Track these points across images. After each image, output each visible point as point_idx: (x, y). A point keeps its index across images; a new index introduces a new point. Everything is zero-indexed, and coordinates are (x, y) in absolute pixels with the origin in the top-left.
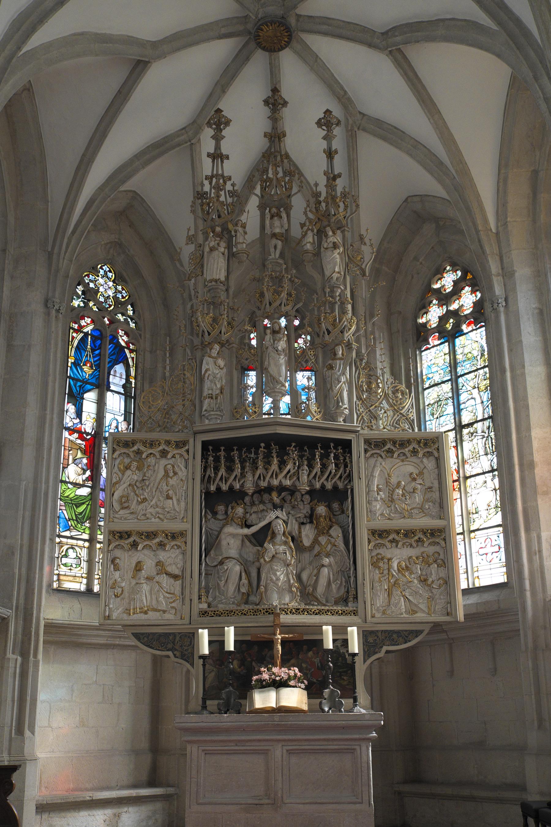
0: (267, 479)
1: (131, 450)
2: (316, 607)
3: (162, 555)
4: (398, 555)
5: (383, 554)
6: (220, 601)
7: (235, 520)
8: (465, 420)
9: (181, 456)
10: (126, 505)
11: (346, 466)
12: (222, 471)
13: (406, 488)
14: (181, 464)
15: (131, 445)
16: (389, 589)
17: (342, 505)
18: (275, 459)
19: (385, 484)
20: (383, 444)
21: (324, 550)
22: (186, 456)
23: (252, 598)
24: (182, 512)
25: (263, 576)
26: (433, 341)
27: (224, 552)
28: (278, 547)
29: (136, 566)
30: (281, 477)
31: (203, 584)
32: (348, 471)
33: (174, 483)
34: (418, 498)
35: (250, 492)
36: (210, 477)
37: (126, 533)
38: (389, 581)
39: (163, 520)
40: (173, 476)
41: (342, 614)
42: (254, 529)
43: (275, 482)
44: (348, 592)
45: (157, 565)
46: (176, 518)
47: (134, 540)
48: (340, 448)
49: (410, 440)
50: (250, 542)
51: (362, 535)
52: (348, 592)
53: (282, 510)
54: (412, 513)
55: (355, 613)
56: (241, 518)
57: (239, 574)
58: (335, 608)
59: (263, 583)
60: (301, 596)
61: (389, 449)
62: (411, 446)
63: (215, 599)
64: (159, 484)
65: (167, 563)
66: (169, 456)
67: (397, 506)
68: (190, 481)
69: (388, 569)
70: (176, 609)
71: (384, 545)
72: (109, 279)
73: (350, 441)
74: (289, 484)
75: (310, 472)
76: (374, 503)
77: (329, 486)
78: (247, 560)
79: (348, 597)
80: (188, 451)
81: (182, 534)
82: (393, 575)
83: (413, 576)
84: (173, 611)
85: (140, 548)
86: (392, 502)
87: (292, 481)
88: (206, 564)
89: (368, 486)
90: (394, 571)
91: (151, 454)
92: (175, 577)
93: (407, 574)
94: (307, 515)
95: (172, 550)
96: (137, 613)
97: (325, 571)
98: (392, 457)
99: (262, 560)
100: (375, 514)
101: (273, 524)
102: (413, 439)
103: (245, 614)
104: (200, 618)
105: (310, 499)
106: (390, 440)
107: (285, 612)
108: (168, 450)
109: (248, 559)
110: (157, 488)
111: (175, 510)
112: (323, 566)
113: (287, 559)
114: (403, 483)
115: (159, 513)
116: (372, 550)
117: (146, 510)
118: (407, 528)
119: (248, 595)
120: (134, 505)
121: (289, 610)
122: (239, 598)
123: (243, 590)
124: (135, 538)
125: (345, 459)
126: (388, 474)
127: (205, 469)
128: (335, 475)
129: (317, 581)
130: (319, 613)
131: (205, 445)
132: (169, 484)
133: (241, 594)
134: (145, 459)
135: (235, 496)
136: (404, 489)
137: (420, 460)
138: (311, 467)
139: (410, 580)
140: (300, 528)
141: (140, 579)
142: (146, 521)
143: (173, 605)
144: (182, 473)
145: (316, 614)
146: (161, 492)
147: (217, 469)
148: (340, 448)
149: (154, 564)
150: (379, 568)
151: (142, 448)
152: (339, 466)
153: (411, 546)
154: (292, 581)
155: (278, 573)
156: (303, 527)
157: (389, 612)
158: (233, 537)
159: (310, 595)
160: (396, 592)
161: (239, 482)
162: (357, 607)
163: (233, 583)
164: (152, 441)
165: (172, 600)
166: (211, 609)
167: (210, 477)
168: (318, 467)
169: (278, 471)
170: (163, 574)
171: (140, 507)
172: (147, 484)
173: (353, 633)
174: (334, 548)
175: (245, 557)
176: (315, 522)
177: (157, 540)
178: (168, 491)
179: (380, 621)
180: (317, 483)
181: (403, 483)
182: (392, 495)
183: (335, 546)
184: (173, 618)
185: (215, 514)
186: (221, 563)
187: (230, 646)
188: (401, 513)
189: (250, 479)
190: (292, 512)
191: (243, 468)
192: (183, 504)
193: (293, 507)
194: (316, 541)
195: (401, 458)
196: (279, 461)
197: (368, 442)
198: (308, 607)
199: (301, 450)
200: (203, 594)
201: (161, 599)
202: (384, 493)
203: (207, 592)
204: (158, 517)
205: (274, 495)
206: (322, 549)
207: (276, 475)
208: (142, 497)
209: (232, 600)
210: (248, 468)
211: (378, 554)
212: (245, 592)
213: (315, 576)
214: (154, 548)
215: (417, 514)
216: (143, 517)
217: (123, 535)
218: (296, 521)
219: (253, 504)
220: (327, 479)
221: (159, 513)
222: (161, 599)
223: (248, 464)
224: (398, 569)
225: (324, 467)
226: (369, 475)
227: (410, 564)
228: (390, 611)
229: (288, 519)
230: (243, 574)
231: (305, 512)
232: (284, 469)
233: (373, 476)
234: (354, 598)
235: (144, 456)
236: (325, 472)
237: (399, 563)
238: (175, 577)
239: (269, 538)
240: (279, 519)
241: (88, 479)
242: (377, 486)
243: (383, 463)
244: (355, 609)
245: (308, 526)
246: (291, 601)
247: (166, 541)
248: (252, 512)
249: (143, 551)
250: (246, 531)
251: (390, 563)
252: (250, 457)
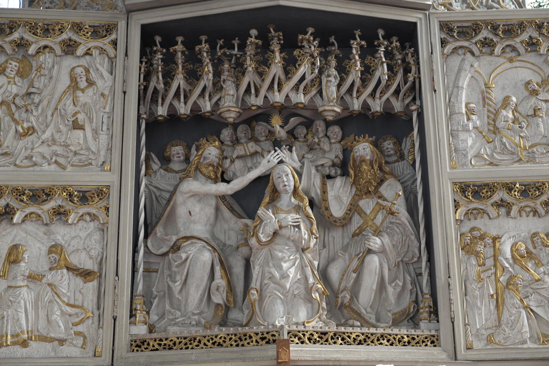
0: (263, 92)
1: (8, 39)
2: (358, 330)
3: (61, 233)
5: (483, 230)
6: (172, 320)
7: (203, 170)
9: (102, 51)
11: (407, 71)
13: (519, 109)
14: (100, 64)
15: (8, 30)
16: (497, 293)
17: (400, 144)
18: (277, 54)
19: (481, 102)
20: (475, 30)
21: (370, 223)
22: (111, 51)
23: (234, 315)
24: (103, 153)
25: (256, 271)
27: (182, 229)
28: (284, 216)
29: (9, 254)
30: (288, 87)
31: (140, 287)
32: (411, 79)
33: (90, 101)
35: (231, 117)
36: (156, 91)
38: (497, 280)
39: (64, 168)
40: (87, 87)
41: (409, 342)
42: (239, 183)
43: (278, 98)
44: (416, 302)
45: (50, 252)
46: (91, 164)
47: (7, 205)
48: (395, 39)
49: (522, 23)
50: (232, 210)
51: (443, 193)
52: (416, 302)
53: (290, 150)
54: (533, 152)
55: (434, 341)
56: (213, 166)
57: (210, 266)
58: (396, 331)
59: (255, 283)
60: (328, 311)
61: (485, 39)
62: (525, 33)
63: (162, 317)
64: (60, 100)
65: (71, 248)
66: (80, 51)
67: (504, 140)
68: (119, 95)
69: (494, 256)
70: (85, 338)
71: (484, 212)
73: (415, 24)
74: (303, 101)
76: (462, 136)
77: (377, 106)
78: (225, 245)
80: (114, 43)
81: (101, 193)
82: (504, 268)
83: (542, 269)
84: (80, 341)
85: (17, 218)
86: (494, 133)
87: (308, 97)
88: (147, 251)
89: (449, 104)
90: (506, 259)
91: (45, 47)
92: (86, 275)
93: (530, 265)
94: (337, 161)
95: (81, 223)
96: (7, 345)
97: (374, 261)
98: (492, 53)
99: (253, 241)
100: (465, 156)
101: (275, 175)
102: (529, 22)
103: (220, 345)
104: (131, 354)
105: (340, 134)
106: (486, 23)
107: (300, 339)
108: (78, 40)
109: (228, 243)
110: (56, 109)
111: (88, 149)
112: (370, 251)
113: (301, 238)
114: (514, 99)
115: (57, 155)
116: (461, 221)
117: (32, 149)
118: (528, 180)
119: (227, 309)
121: (307, 335)
122: (209, 313)
123: (218, 299)
124: (8, 200)
125: (404, 60)
126: (485, 84)
127: (147, 76)
128: (388, 87)
129: (358, 282)
130: (364, 341)
131: (148, 33)
132: (78, 101)
133: (213, 307)
134: (33, 56)
135: (204, 125)
136: (515, 110)
137: (543, 58)
138: (343, 71)
139: (537, 277)
140: (324, 184)
141: (15, 278)
142: (31, 169)
143: (80, 328)
144: (104, 82)
145: (360, 343)
146: (62, 117)
147: (168, 76)
148: (395, 39)
149: (44, 250)
150: (477, 254)
151: (28, 37)
152: (395, 70)
153: (535, 212)
154: (311, 280)
155: (285, 265)
156: (329, 183)
157: (499, 338)
158: (199, 201)
159: (346, 307)
160: (512, 300)
161: (210, 99)
162: (437, 330)
163: (198, 286)
164: (48, 25)
165: (77, 320)
166: (154, 335)
167: (156, 91)
168: (355, 74)
169: (283, 77)
170: (61, 268)
171: (21, 143)
172: (37, 100)
174: (390, 218)
175: (222, 237)
176: (352, 172)
177: (52, 204)
178: (76, 113)
179: (483, 357)
180: (355, 101)
181: (514, 99)
182: (494, 121)
183: (392, 213)
184: (78, 354)
185: (165, 160)
186: (176, 248)
188: (513, 154)
189: (231, 92)
190: (309, 156)
191: (217, 74)
192: (104, 138)
193: (311, 149)
194: (354, 208)
195: (508, 56)
196: (284, 59)
197: (446, 27)
198: (342, 329)
199: (324, 44)
200: (139, 307)
201: (56, 316)
202: (479, 118)
203: (148, 304)
204: (56, 162)
205: (276, 122)
206: (366, 222)
207: (280, 85)
208: (25, 125)
209: (196, 317)
210: (226, 73)
211: (473, 229)
212: (221, 302)
213: (354, 271)
214: (45, 218)
215: (543, 154)
216: (26, 162)
218: (317, 171)
219: (236, 142)
220: (373, 95)
221: (57, 155)
222: (56, 316)
223: (226, 66)
224: (513, 257)
225: (367, 71)
226: (451, 85)
227: (535, 248)
228: (501, 336)
229: (302, 167)
230: (218, 268)
231: (332, 156)
232: (294, 74)
233: (458, 87)
234: (430, 313)
235: (32, 50)
236: (370, 80)
237: (514, 245)
238: (86, 275)
239: (267, 199)
240: (285, 166)
242: (467, 105)
243: (476, 65)
244: (433, 333)
245: (339, 181)
246: (310, 318)
247: (68, 206)
248: (234, 156)
249: (24, 226)
250: (223, 188)
251: (497, 244)
252: (231, 56)
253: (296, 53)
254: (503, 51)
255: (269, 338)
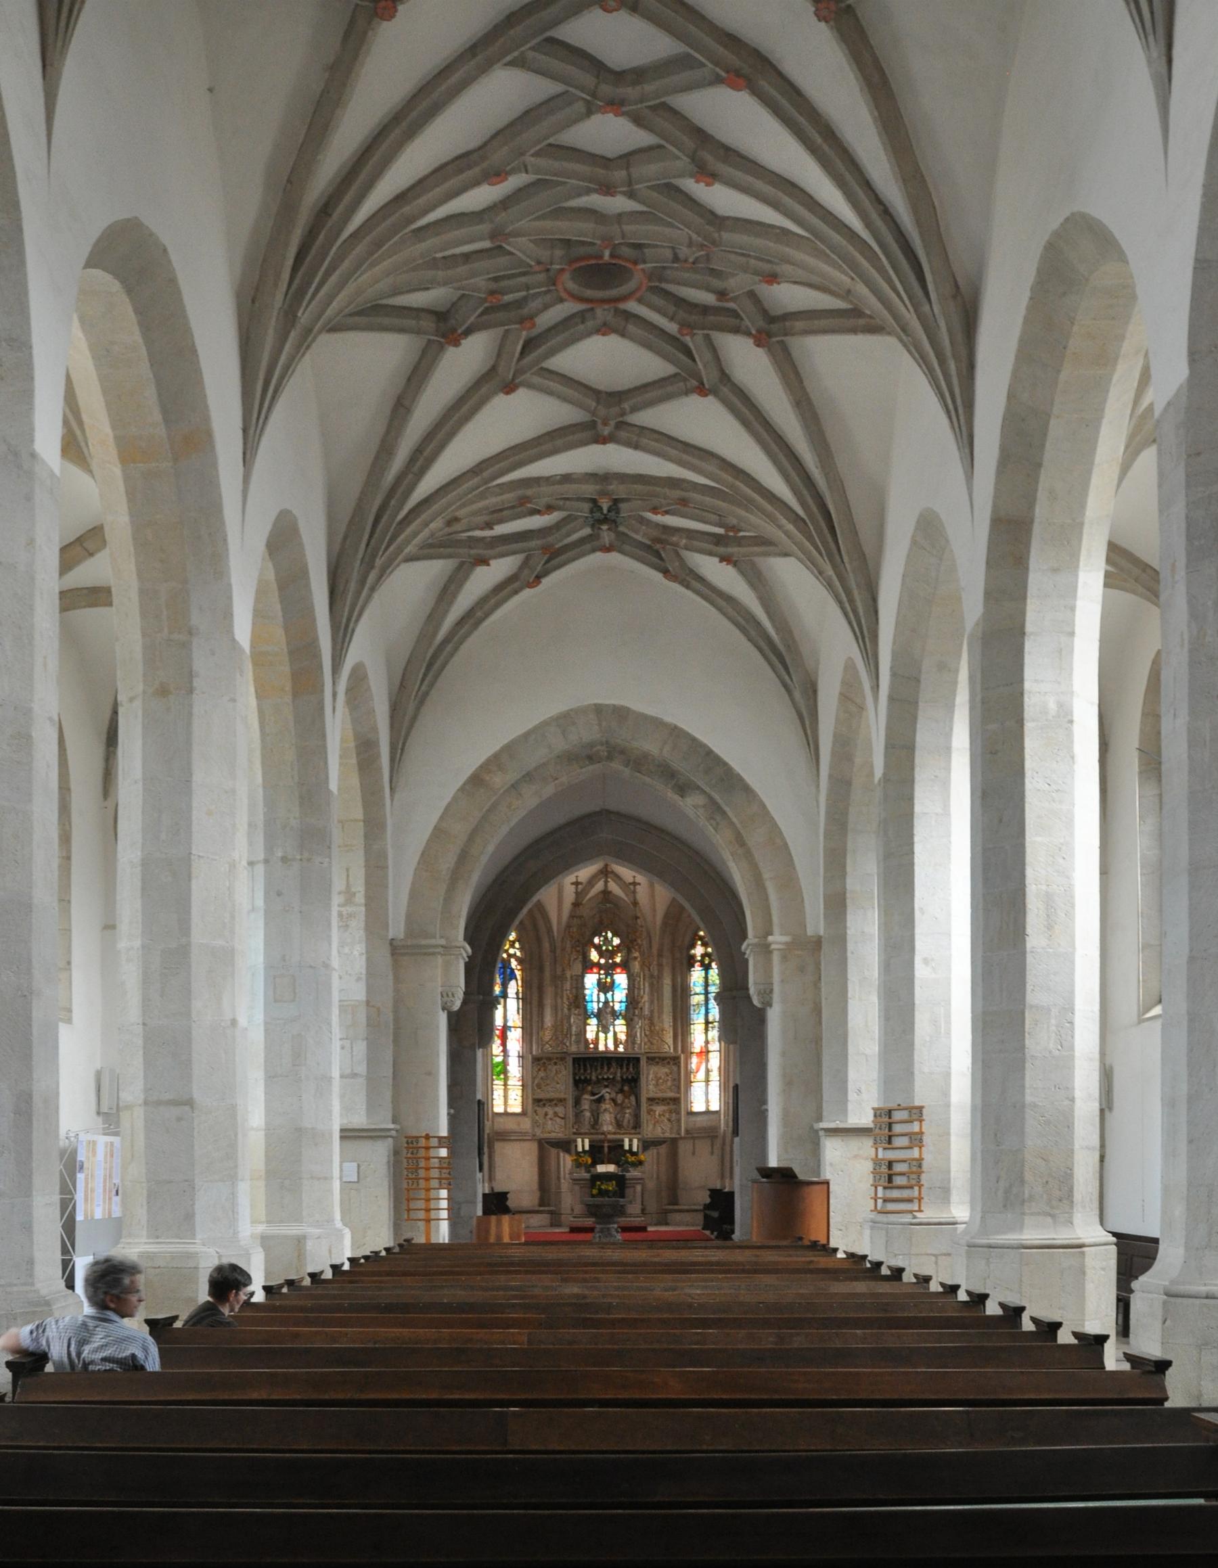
3: (557, 1109)
4: (659, 1109)
8: (711, 1019)
26: (697, 967)
34: (669, 1083)
51: (643, 1100)
79: (637, 1125)
131: (574, 1059)
173: (635, 1142)
187: (587, 1148)
217: (539, 1100)
240: (605, 1092)
255: (603, 1134)
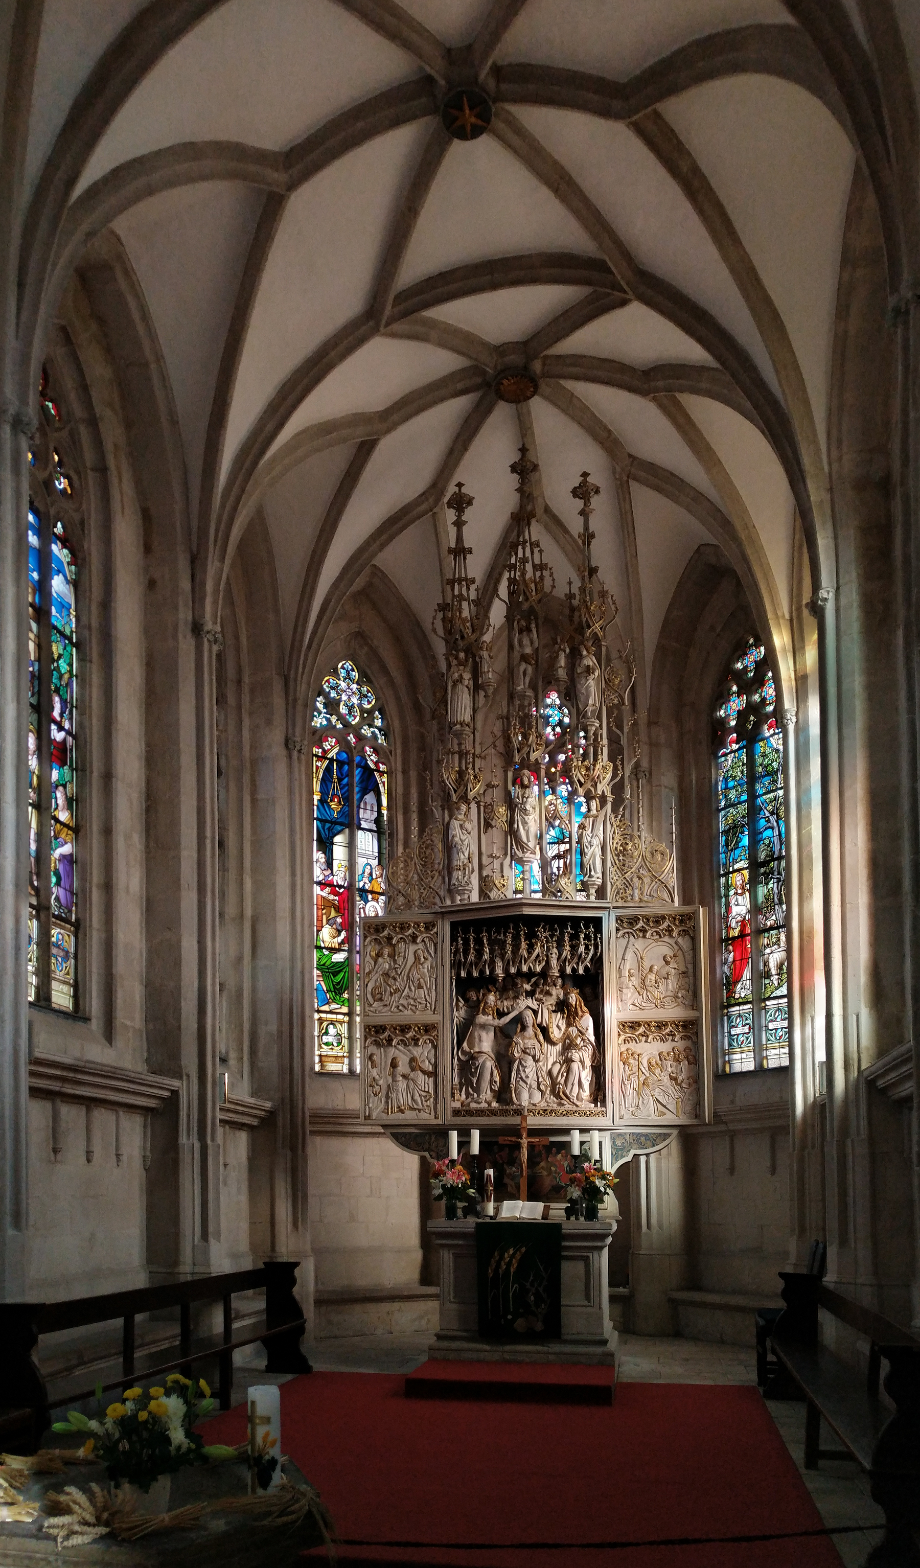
10: (378, 996)
11: (596, 948)
12: (471, 957)
37: (381, 1026)
72: (352, 681)
75: (560, 955)
88: (459, 1059)
111: (426, 1000)
120: (386, 998)
149: (408, 1060)
199: (552, 930)
201: (417, 1097)
225: (574, 948)
241: (343, 942)
253: (533, 941)
254: (652, 935)
